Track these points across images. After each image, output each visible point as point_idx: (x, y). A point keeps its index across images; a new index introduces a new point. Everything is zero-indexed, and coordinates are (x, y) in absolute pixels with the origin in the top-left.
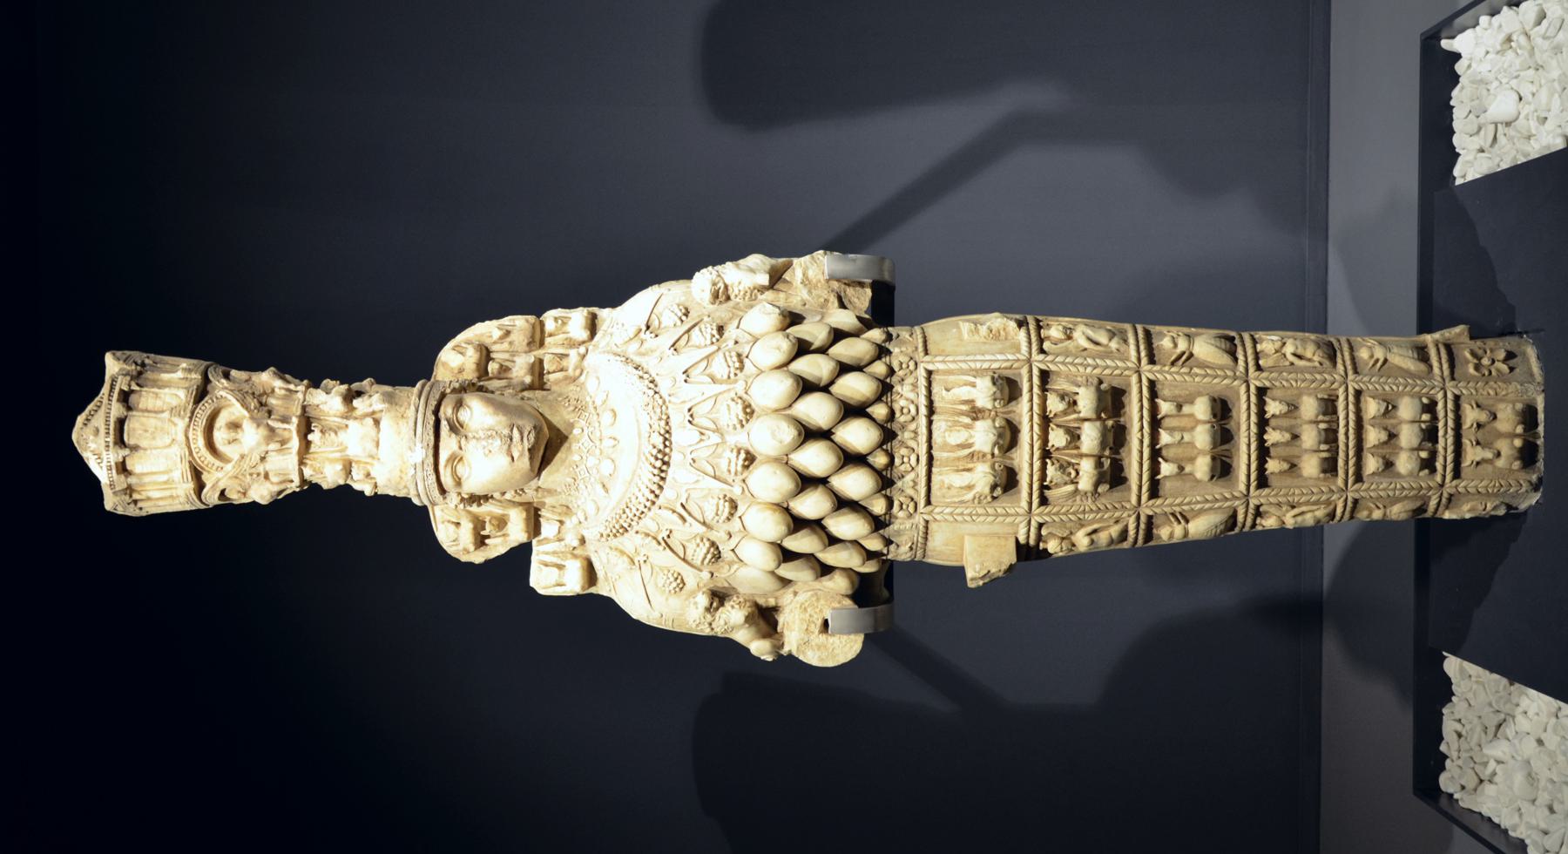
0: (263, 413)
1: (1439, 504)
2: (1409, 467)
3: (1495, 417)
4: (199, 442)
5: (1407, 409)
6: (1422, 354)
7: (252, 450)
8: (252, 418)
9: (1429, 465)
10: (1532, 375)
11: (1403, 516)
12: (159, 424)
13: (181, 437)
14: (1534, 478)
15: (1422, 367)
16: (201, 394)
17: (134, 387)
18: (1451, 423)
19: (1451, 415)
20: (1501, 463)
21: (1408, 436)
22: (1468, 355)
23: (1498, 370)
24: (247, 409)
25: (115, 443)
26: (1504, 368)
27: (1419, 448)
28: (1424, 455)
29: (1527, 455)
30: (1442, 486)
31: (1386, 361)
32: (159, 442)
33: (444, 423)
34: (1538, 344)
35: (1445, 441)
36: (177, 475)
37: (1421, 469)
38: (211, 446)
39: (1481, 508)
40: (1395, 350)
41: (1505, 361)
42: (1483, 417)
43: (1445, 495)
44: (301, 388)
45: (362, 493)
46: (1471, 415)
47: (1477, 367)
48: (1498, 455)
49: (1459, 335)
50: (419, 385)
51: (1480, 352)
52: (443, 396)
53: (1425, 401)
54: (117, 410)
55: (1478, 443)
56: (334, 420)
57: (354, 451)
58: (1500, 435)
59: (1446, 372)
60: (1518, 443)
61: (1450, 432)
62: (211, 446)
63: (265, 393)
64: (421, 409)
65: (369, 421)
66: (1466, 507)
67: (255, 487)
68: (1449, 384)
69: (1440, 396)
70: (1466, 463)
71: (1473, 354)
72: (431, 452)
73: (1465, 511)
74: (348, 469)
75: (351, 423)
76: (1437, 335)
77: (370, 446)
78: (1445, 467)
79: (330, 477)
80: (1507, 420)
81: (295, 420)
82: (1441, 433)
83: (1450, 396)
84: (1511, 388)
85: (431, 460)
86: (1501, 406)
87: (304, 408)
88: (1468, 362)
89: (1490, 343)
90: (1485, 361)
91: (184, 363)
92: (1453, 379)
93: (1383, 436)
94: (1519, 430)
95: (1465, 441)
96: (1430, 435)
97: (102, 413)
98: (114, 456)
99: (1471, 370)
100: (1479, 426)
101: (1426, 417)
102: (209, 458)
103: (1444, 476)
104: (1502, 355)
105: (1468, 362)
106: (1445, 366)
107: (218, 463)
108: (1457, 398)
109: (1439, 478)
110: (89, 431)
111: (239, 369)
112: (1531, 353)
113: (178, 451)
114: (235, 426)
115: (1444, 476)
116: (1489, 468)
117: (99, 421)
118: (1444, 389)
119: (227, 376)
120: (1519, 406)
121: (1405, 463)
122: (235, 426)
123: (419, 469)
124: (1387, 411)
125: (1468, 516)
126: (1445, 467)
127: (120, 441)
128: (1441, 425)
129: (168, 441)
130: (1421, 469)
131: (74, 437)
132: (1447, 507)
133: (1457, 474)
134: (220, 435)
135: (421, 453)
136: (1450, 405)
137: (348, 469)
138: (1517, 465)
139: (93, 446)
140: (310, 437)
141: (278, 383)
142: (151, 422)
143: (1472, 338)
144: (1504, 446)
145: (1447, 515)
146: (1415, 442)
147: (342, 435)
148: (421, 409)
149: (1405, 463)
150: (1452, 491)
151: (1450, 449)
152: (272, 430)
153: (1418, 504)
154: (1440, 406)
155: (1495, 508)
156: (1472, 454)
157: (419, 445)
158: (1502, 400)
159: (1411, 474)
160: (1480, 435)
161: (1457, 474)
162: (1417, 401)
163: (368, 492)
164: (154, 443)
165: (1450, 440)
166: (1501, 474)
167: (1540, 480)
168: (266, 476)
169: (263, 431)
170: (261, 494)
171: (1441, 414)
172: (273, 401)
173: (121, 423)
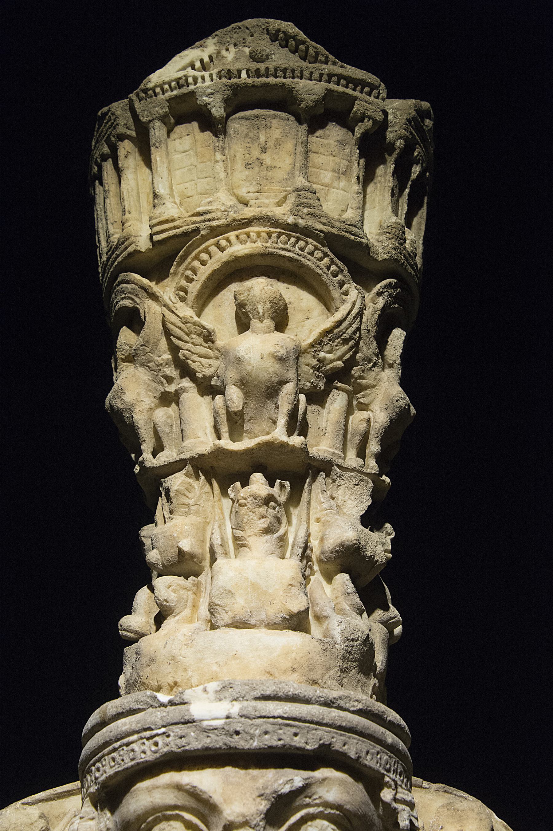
0: (310, 378)
4: (239, 247)
7: (224, 354)
8: (299, 353)
12: (280, 174)
13: (249, 212)
16: (352, 255)
17: (359, 130)
24: (318, 343)
25: (236, 89)
32: (240, 174)
33: (297, 778)
36: (170, 209)
38: (238, 270)
44: (372, 466)
45: (128, 610)
50: (393, 715)
52: (372, 782)
54: (310, 89)
56: (295, 532)
57: (228, 571)
62: (238, 270)
63: (360, 388)
64: (333, 714)
65: (297, 605)
67: (143, 374)
72: (216, 741)
74: (185, 565)
75: (291, 566)
77: (239, 605)
79: (169, 531)
81: (296, 440)
85: (195, 742)
87: (324, 467)
91: (414, 237)
97: (295, 61)
98: (209, 89)
102: (204, 272)
107: (194, 288)
110: (264, 45)
111: (407, 342)
113: (222, 204)
114: (280, 320)
117: (281, 57)
119: (385, 323)
122: (280, 320)
123: (174, 713)
127: (242, 100)
129: (243, 192)
131: (248, 22)
134: (260, 289)
135: (209, 709)
137: (185, 565)
139: (230, 55)
140: (258, 481)
141: (379, 416)
142: (283, 160)
147: (260, 545)
148: (333, 714)
152: (272, 391)
157: (235, 709)
163: (135, 621)
164: (239, 165)
168: (168, 399)
169: (268, 369)
170: (133, 389)
172: (337, 401)
173: (281, 101)
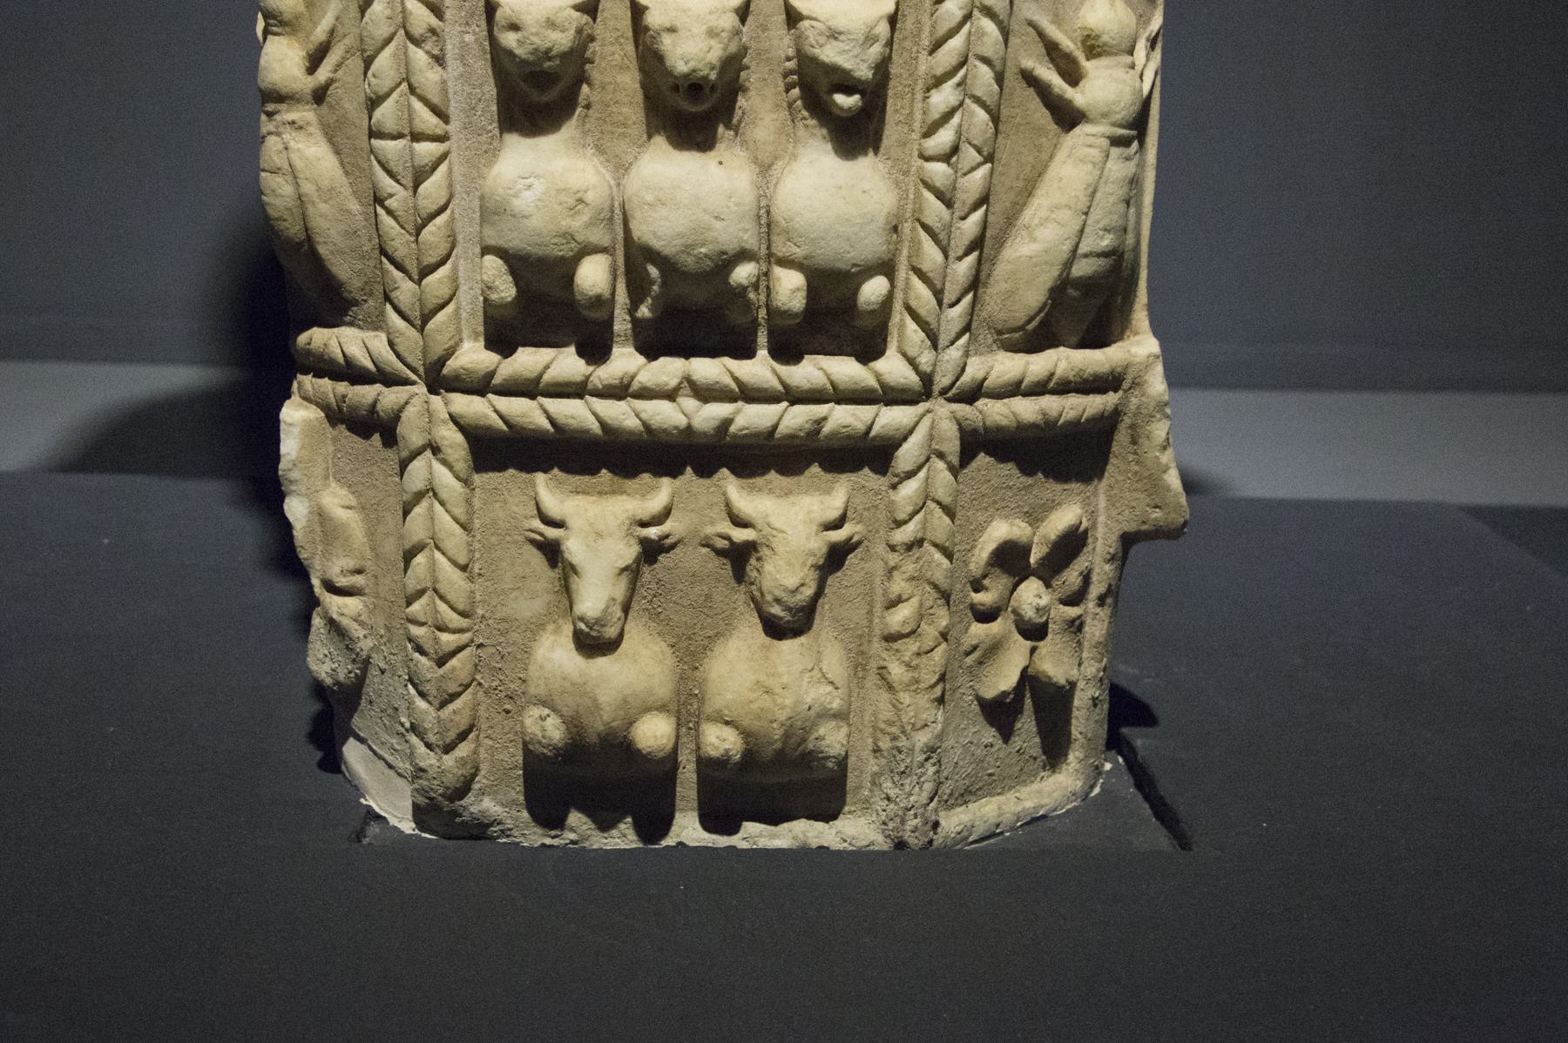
1: (351, 373)
2: (525, 201)
3: (776, 630)
5: (829, 195)
6: (1085, 306)
9: (541, 304)
10: (966, 795)
11: (278, 192)
14: (484, 805)
15: (1032, 298)
18: (752, 417)
19: (796, 418)
20: (556, 655)
21: (689, 195)
22: (1063, 519)
23: (994, 649)
26: (1003, 678)
27: (637, 259)
28: (593, 275)
29: (590, 772)
30: (439, 380)
31: (1067, 117)
34: (1087, 808)
35: (663, 391)
37: (517, 263)
39: (337, 567)
40: (1118, 167)
41: (1028, 679)
42: (785, 573)
43: (390, 397)
46: (791, 518)
47: (1011, 559)
48: (593, 643)
49: (1153, 485)
51: (1071, 577)
53: (873, 290)
55: (651, 551)
58: (691, 653)
59: (995, 412)
60: (654, 733)
61: (708, 415)
66: (337, 501)
68: (943, 418)
69: (892, 368)
70: (550, 491)
71: (1071, 544)
73: (321, 487)
76: (1157, 384)
78: (529, 388)
80: (759, 683)
82: (707, 369)
83: (891, 418)
84: (918, 706)
86: (834, 661)
88: (1034, 517)
89: (1097, 627)
90: (1031, 595)
92: (974, 442)
93: (691, 52)
94: (721, 740)
95: (661, 492)
96: (694, 308)
99: (1001, 530)
100: (739, 557)
101: (790, 287)
103: (481, 386)
104: (1055, 663)
105: (1034, 517)
106: (1027, 409)
108: (874, 454)
109: (473, 355)
112: (1056, 789)
115: (481, 386)
116: (528, 606)
118: (923, 391)
120: (832, 739)
121: (546, 180)
124: (814, 86)
125: (296, 509)
126: (529, 388)
128: (759, 369)
130: (517, 263)
132: (336, 415)
133: (496, 451)
136: (843, 418)
138: (550, 729)
143: (1128, 541)
144: (640, 666)
145: (296, 416)
146: (660, 228)
149: (546, 180)
150: (411, 432)
151: (622, 414)
153: (343, 269)
154: (845, 369)
155: (333, 625)
156: (598, 521)
158: (859, 664)
159: (490, 211)
160: (692, 559)
161: (496, 451)
162: (871, 246)
165: (665, 414)
166: (502, 650)
167: (479, 830)
171: (810, 371)
